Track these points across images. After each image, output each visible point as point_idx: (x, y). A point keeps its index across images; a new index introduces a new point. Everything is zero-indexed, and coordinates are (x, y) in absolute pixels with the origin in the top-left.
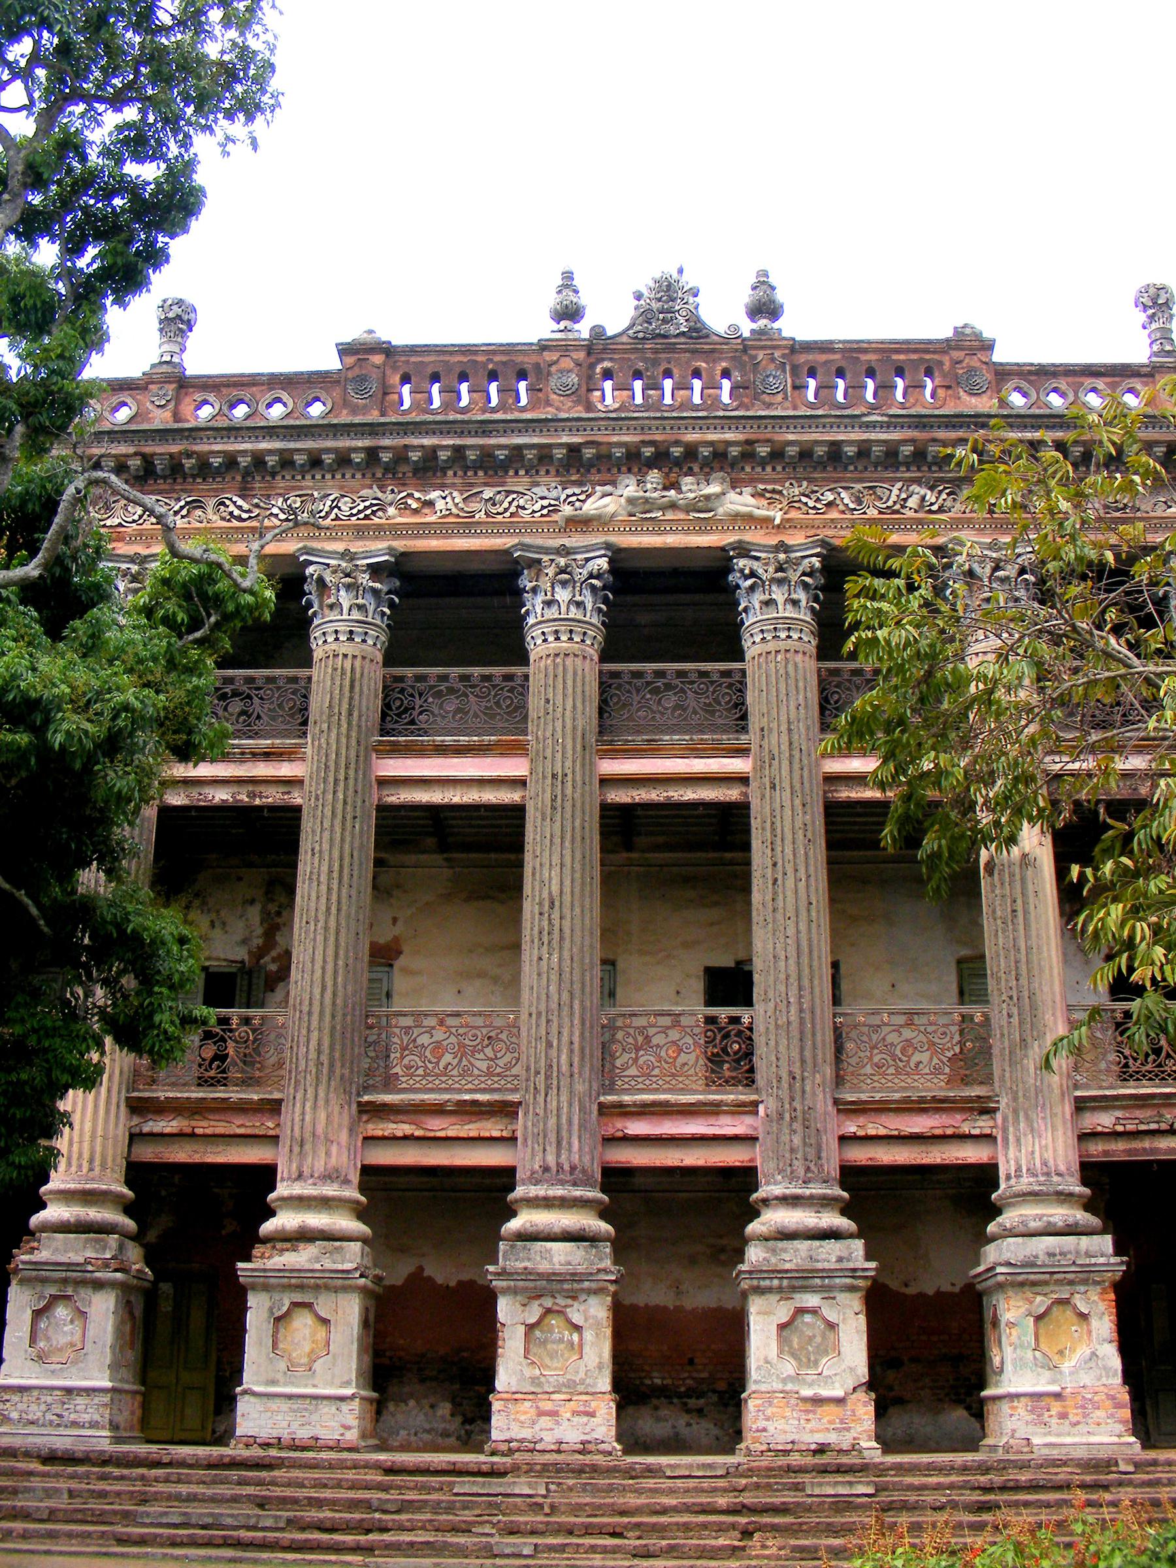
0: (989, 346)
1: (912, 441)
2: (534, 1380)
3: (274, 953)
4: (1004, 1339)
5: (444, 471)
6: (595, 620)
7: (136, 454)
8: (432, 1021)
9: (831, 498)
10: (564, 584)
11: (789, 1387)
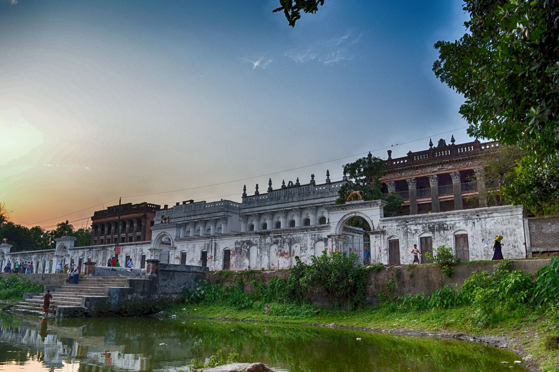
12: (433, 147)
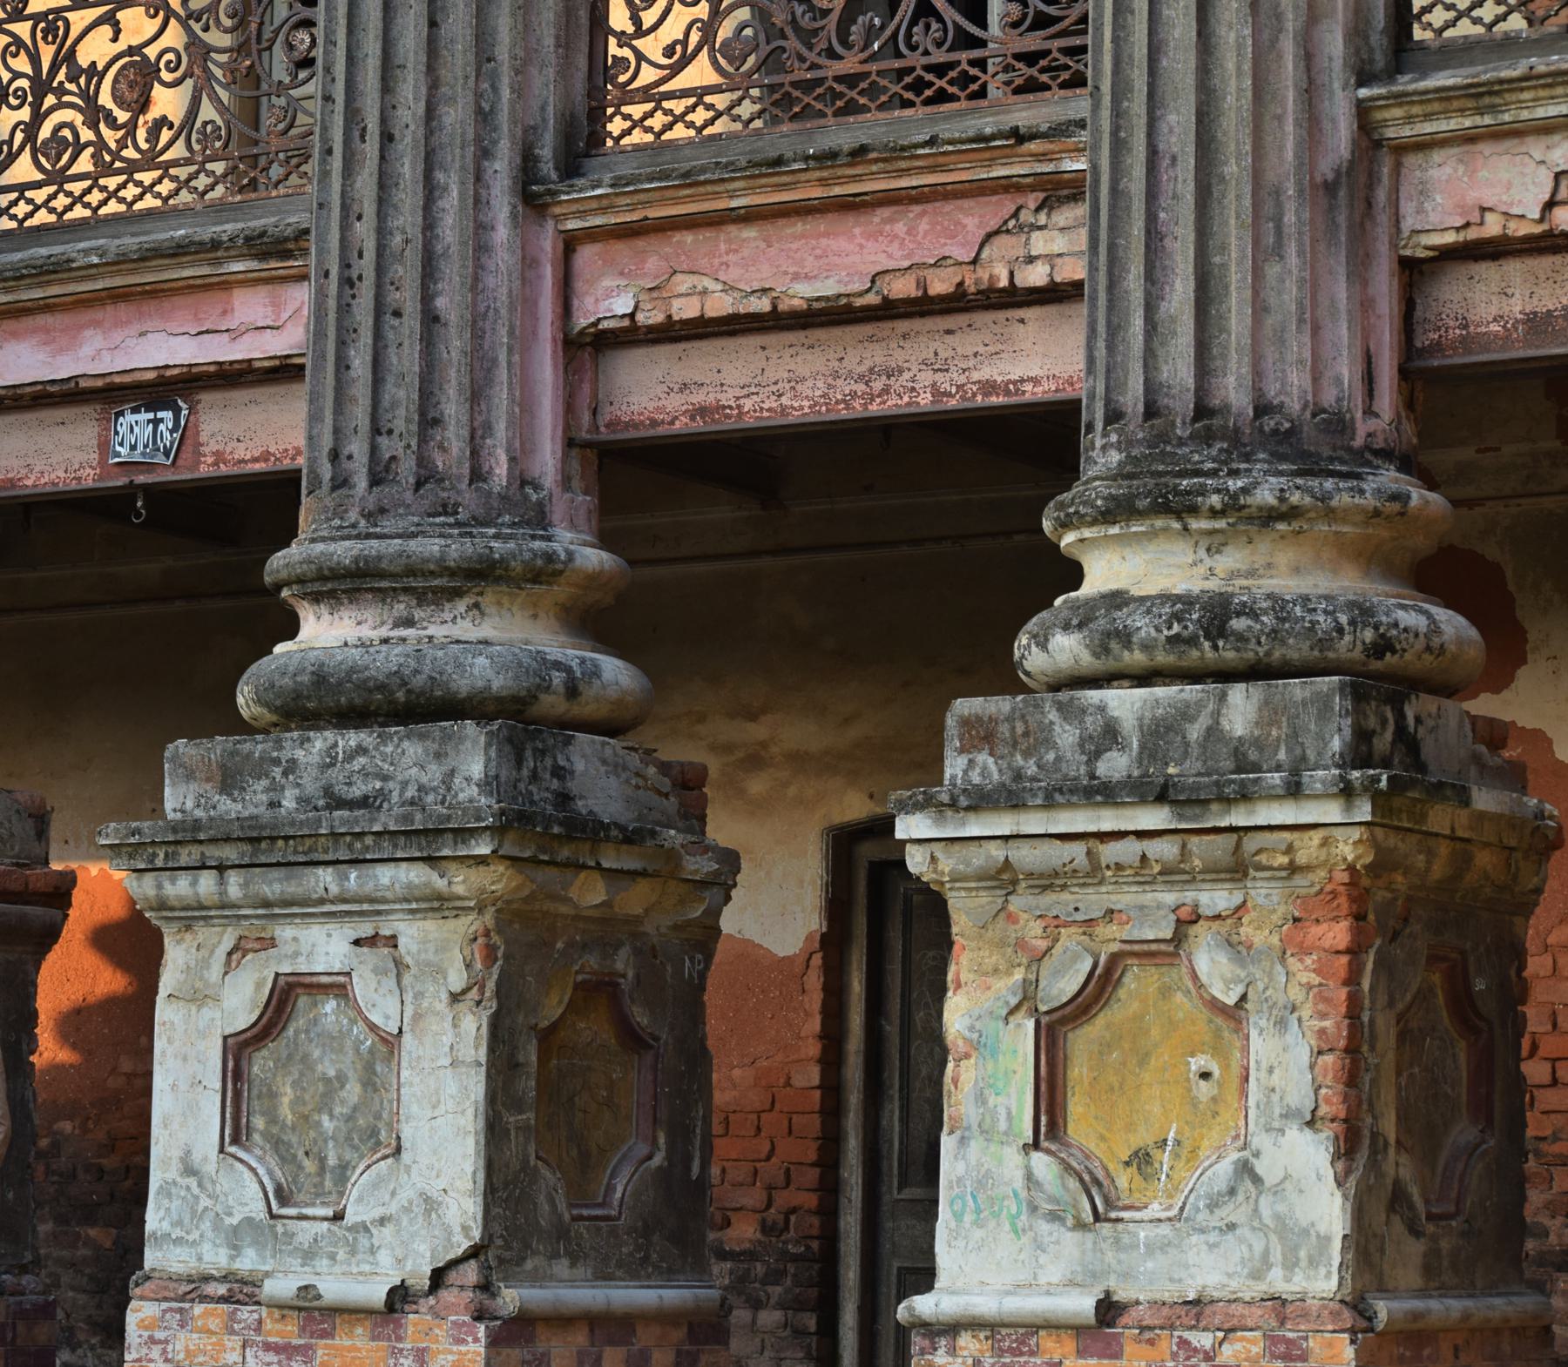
11: (248, 1262)
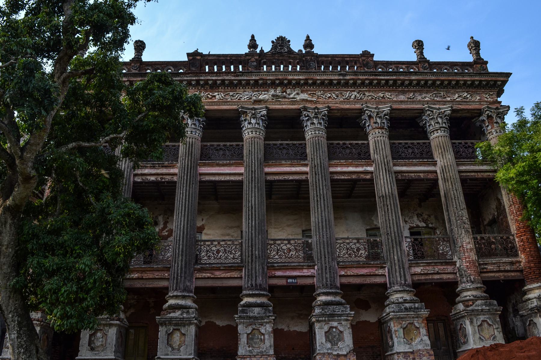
0: (373, 55)
1: (353, 79)
2: (250, 351)
3: (167, 230)
4: (394, 336)
5: (218, 87)
6: (263, 129)
7: (127, 81)
8: (216, 243)
9: (330, 95)
10: (254, 118)
11: (329, 351)
12: (258, 51)
